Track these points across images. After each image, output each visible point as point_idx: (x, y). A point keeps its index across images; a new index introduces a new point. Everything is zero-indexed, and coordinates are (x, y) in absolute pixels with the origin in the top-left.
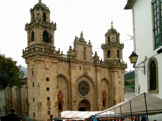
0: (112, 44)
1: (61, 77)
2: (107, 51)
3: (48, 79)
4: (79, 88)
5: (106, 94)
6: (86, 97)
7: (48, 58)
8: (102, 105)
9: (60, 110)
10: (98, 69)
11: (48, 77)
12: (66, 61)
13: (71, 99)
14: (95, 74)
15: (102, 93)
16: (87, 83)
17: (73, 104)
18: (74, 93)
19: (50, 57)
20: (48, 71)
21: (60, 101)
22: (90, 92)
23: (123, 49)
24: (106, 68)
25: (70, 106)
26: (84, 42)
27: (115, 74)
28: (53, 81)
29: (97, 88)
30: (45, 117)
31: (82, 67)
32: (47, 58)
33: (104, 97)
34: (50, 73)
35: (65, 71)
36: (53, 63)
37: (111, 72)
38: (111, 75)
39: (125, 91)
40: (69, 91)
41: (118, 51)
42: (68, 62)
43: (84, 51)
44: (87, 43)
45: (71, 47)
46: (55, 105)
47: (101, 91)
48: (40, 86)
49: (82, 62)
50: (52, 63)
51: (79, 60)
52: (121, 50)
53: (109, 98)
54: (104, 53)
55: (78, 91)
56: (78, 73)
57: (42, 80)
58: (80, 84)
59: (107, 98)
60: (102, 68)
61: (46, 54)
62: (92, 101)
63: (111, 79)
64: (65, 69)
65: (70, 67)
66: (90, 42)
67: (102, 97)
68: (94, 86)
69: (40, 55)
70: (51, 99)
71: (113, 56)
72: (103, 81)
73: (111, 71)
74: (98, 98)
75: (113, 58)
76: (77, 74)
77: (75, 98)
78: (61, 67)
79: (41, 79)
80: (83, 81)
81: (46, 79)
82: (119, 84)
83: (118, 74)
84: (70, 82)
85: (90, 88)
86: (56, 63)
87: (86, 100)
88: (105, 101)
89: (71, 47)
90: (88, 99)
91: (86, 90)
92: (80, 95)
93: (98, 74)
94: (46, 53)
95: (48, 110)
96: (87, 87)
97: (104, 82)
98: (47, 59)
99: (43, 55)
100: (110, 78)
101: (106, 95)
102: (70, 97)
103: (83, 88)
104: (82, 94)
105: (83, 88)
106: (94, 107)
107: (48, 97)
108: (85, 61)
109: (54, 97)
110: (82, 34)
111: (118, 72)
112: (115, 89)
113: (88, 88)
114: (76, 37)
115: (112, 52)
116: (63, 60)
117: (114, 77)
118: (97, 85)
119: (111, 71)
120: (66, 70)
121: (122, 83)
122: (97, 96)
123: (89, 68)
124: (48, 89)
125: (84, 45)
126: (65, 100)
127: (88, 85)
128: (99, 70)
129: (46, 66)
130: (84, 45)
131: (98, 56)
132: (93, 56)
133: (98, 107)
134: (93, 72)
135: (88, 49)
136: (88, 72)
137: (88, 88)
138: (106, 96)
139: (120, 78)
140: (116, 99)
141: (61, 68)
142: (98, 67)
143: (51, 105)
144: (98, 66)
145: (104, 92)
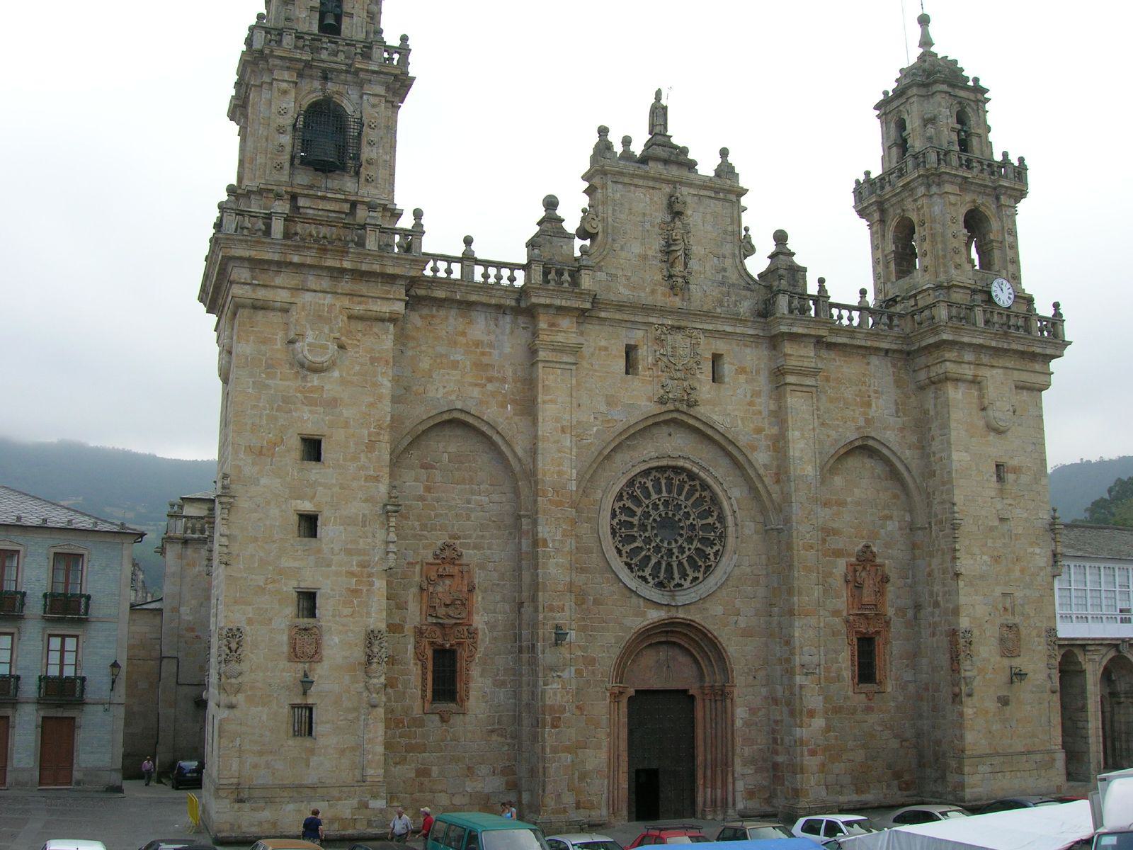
0: (917, 166)
1: (459, 432)
2: (892, 224)
3: (313, 449)
4: (631, 525)
5: (885, 580)
6: (682, 598)
7: (325, 283)
8: (847, 674)
10: (792, 362)
11: (311, 430)
12: (499, 308)
13: (536, 610)
14: (765, 404)
15: (841, 566)
16: (705, 486)
17: (547, 656)
18: (555, 569)
20: (315, 380)
21: (442, 626)
22: (724, 559)
23: (1022, 206)
24: (875, 360)
25: (525, 669)
26: (666, 162)
27: (947, 405)
28: (355, 458)
29: (787, 521)
30: (261, 753)
31: (645, 355)
32: (312, 282)
33: (868, 597)
34: (333, 403)
35: (490, 387)
36: (360, 318)
37: (922, 388)
38: (926, 412)
39: (1059, 550)
40: (525, 544)
41: (975, 223)
42: (517, 311)
43: (666, 228)
44: (707, 167)
45: (551, 203)
46: (363, 659)
47: (838, 553)
48: (243, 503)
49: (647, 309)
50: (360, 326)
51: (623, 292)
52: (1000, 207)
53: (918, 607)
54: (875, 247)
55: (612, 554)
56: (611, 401)
57: (261, 453)
58: (632, 491)
59: (901, 611)
60: (824, 353)
61: (296, 259)
62: (747, 633)
63: (923, 446)
64: (490, 373)
65: (533, 352)
66: (730, 159)
67: (842, 602)
68: (763, 511)
69: (256, 264)
70: (324, 607)
71: (928, 261)
72: (853, 462)
73: (922, 376)
74: (791, 613)
75: (927, 277)
76: (603, 408)
77: (569, 602)
78: (458, 357)
79: (250, 449)
81: (296, 443)
82: (996, 485)
83: (981, 397)
84: (531, 475)
85: (730, 520)
86: (393, 319)
87: (689, 625)
88: (879, 641)
89: (551, 203)
90: (712, 617)
91: (696, 544)
92: (633, 584)
93: (796, 402)
94: (297, 248)
95: (298, 701)
96: (710, 513)
97: (863, 468)
98: (308, 297)
99: (281, 265)
100: (914, 439)
101: (890, 588)
102: (525, 594)
103: (667, 524)
104: (655, 574)
105: (667, 524)
106: (764, 691)
107: (307, 585)
108: (677, 302)
109: (355, 592)
110: (658, 114)
111: (975, 382)
112: (955, 527)
113: (710, 520)
114: (603, 131)
115: (922, 224)
116: (473, 298)
117: (945, 426)
118: (786, 498)
119: (922, 376)
120: (504, 380)
121: (1024, 479)
122: (790, 592)
123: (716, 359)
124: (309, 523)
125: (668, 182)
126: (492, 626)
127: (709, 503)
128: (799, 373)
129: (298, 345)
130: (668, 182)
131: (798, 260)
132: (757, 265)
133: (791, 686)
134: (756, 394)
135: (700, 218)
136: (705, 389)
137: (710, 520)
138: (880, 592)
139: (999, 432)
140: (964, 623)
141: (455, 366)
142: (788, 348)
143: (326, 652)
144: (793, 337)
145: (866, 558)
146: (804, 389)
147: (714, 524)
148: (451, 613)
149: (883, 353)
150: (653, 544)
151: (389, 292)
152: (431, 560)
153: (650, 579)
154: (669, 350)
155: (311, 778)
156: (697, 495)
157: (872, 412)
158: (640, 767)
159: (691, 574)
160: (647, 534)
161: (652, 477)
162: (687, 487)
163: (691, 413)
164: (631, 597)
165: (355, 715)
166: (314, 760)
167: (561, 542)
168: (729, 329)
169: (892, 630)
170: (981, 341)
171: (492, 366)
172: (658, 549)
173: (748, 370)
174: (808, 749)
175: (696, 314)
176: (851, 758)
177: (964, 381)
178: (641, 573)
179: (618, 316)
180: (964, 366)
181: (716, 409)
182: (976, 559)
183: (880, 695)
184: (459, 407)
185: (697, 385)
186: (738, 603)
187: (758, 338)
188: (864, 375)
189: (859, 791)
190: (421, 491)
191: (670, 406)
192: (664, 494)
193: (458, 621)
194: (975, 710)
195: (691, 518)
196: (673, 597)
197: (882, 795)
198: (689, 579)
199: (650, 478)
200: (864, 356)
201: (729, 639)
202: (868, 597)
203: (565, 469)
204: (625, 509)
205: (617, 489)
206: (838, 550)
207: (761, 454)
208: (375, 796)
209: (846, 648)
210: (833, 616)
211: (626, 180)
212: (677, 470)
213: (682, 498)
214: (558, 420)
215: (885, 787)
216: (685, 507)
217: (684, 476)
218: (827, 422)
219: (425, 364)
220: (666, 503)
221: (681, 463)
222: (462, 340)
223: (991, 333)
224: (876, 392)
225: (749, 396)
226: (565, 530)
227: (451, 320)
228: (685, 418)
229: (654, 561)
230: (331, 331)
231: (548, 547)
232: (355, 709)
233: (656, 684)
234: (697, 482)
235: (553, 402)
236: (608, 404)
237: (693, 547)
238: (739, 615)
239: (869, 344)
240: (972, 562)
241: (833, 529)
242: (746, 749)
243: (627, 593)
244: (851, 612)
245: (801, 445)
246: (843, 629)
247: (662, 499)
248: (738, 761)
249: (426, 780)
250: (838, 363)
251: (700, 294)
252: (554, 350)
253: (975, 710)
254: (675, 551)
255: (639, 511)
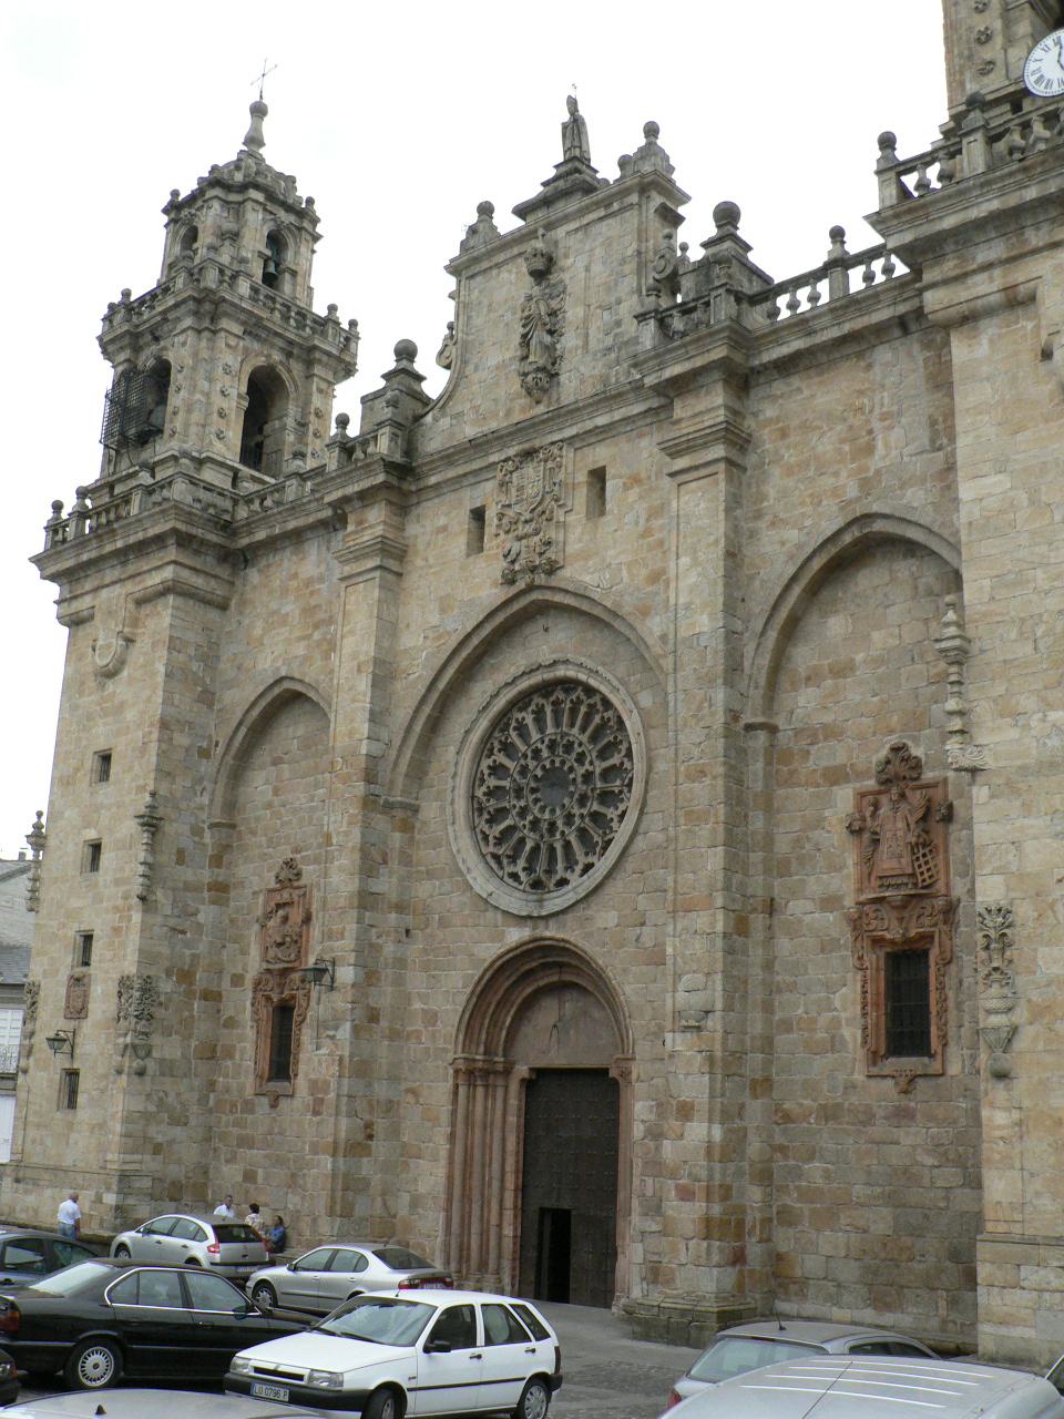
6: (556, 901)
8: (851, 1034)
9: (279, 1086)
11: (102, 745)
15: (844, 800)
16: (607, 704)
19: (123, 555)
35: (317, 636)
72: (869, 580)
78: (288, 608)
80: (545, 689)
95: (67, 1066)
104: (529, 869)
105: (554, 778)
141: (284, 620)
143: (91, 1006)
146: (703, 472)
147: (622, 764)
148: (280, 955)
149: (897, 332)
150: (530, 818)
151: (162, 558)
152: (273, 884)
153: (523, 876)
154: (514, 492)
155: (68, 1162)
156: (597, 719)
157: (877, 462)
158: (547, 1204)
159: (582, 860)
160: (522, 803)
161: (533, 707)
162: (583, 709)
163: (553, 584)
164: (486, 910)
165: (104, 1083)
166: (74, 1137)
167: (346, 834)
168: (601, 421)
169: (962, 929)
170: (995, 205)
171: (318, 606)
172: (535, 824)
173: (643, 475)
174: (677, 1186)
175: (543, 422)
176: (861, 1223)
177: (990, 312)
178: (511, 869)
179: (451, 473)
180: (970, 281)
181: (591, 562)
182: (1027, 727)
183: (932, 1082)
184: (284, 674)
185: (552, 534)
186: (642, 901)
187: (658, 414)
188: (861, 393)
189: (879, 1302)
190: (269, 796)
191: (521, 585)
192: (550, 730)
193: (286, 965)
194: (1016, 1115)
195: (587, 762)
196: (540, 901)
197: (934, 1323)
198: (578, 869)
199: (530, 709)
200: (860, 355)
201: (624, 970)
202: (892, 859)
203: (356, 725)
204: (496, 770)
205: (475, 737)
206: (836, 768)
207: (658, 619)
208: (108, 1189)
209: (850, 975)
210: (823, 910)
211: (485, 265)
212: (568, 684)
213: (575, 731)
214: (354, 656)
215: (942, 1303)
216: (580, 745)
217: (579, 692)
218: (782, 515)
219: (258, 632)
220: (552, 746)
221: (561, 672)
222: (294, 584)
223: (1011, 174)
224: (884, 417)
225: (642, 521)
226: (351, 816)
227: (286, 564)
228: (548, 596)
229: (529, 845)
230: (116, 625)
231: (332, 845)
232: (105, 1076)
233: (558, 1059)
234: (597, 699)
235: (352, 632)
236: (443, 611)
237: (585, 811)
238: (643, 924)
239: (847, 328)
240: (1014, 734)
241: (824, 726)
242: (650, 1181)
243: (482, 905)
244: (863, 898)
245: (692, 579)
246: (847, 936)
247: (547, 740)
248: (635, 1203)
249: (251, 1187)
250: (806, 393)
251: (573, 384)
252: (357, 559)
253: (1016, 1115)
254: (560, 823)
255: (510, 764)
